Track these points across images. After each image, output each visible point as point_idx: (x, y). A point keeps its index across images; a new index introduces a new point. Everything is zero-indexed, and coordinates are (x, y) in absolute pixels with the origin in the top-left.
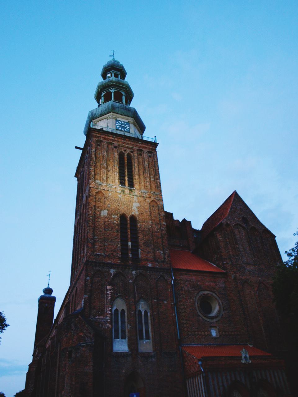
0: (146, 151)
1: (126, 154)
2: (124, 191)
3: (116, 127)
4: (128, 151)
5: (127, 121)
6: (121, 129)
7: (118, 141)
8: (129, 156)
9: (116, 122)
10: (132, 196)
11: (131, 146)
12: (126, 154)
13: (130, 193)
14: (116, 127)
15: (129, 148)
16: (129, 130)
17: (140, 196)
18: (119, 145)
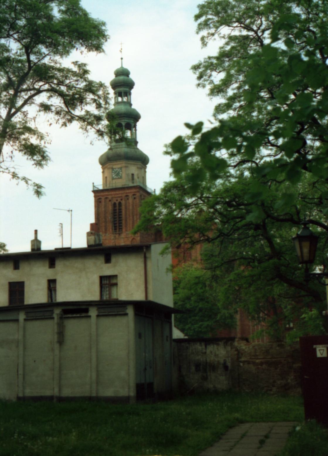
0: (130, 195)
1: (117, 203)
2: (115, 237)
4: (119, 200)
5: (119, 166)
7: (111, 195)
8: (120, 203)
11: (120, 195)
12: (117, 203)
15: (119, 197)
18: (112, 198)
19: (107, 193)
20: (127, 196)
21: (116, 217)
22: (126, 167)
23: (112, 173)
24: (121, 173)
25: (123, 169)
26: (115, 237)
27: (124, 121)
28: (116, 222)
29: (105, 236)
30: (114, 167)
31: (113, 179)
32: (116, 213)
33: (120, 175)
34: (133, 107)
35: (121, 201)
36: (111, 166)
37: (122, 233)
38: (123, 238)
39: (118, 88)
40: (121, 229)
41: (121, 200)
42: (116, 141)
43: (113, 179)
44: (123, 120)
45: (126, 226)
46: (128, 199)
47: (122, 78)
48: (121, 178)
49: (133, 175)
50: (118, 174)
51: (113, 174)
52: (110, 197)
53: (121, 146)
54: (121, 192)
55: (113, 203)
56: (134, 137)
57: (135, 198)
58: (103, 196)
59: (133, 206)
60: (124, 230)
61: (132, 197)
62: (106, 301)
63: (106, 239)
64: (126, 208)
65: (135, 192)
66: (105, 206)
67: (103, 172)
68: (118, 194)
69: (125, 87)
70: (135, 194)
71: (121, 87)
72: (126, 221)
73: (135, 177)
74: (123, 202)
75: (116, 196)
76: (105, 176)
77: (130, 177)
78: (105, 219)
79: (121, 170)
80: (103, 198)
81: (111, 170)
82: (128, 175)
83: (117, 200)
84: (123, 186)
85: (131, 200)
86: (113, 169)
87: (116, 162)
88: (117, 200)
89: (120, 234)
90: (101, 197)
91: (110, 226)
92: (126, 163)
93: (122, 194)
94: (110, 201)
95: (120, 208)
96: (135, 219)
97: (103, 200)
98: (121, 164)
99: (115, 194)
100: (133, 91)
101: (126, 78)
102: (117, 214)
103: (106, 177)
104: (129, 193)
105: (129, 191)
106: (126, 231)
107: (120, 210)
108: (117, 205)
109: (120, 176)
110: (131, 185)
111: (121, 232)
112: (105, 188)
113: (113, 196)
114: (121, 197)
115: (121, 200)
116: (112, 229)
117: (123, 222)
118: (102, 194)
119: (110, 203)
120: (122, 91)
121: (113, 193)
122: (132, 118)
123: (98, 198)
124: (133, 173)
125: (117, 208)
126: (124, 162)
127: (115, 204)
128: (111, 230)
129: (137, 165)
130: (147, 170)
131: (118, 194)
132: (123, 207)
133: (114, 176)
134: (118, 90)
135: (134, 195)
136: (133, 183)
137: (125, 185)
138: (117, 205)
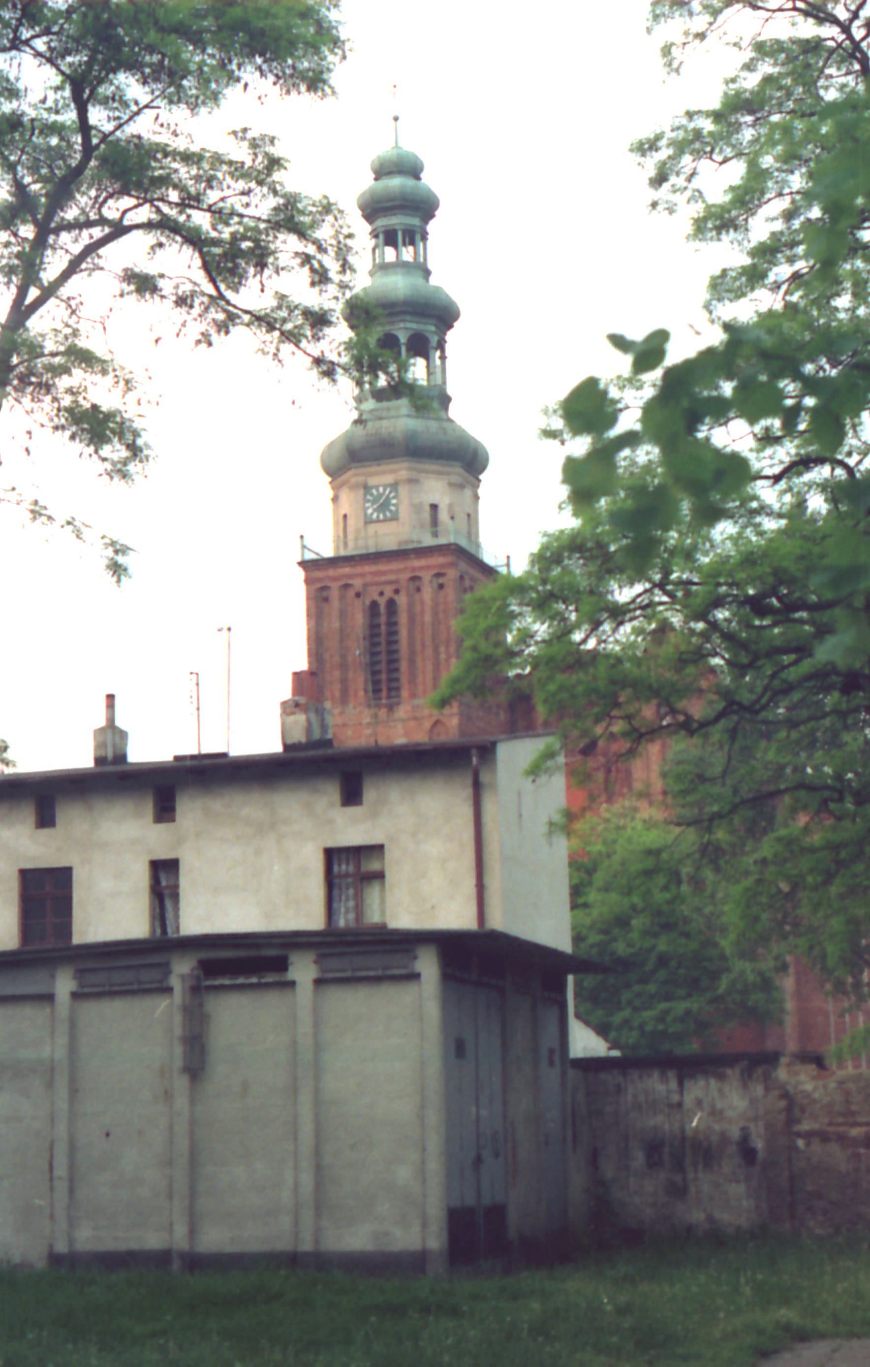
0: (427, 576)
1: (382, 602)
2: (376, 716)
3: (365, 514)
4: (388, 591)
5: (389, 479)
6: (378, 516)
7: (362, 575)
8: (391, 603)
9: (365, 495)
10: (392, 724)
11: (392, 577)
12: (382, 602)
13: (388, 717)
14: (365, 514)
15: (390, 583)
16: (397, 511)
17: (408, 719)
18: (365, 586)
19: (347, 570)
20: (414, 579)
21: (378, 649)
22: (412, 481)
23: (366, 501)
24: (394, 501)
25: (403, 490)
26: (376, 716)
27: (407, 329)
28: (377, 668)
29: (342, 713)
30: (372, 481)
31: (368, 521)
32: (379, 635)
33: (393, 508)
34: (434, 281)
35: (396, 597)
36: (361, 479)
37: (398, 704)
38: (402, 720)
39: (385, 216)
40: (394, 689)
41: (397, 591)
42: (379, 395)
43: (368, 521)
44: (402, 325)
45: (412, 681)
46: (418, 590)
47: (395, 182)
48: (395, 518)
49: (434, 507)
50: (384, 506)
51: (368, 505)
52: (357, 583)
53: (392, 413)
54: (394, 566)
55: (368, 602)
56: (439, 381)
57: (441, 586)
58: (335, 579)
59: (435, 614)
60: (405, 693)
61: (431, 582)
62: (347, 932)
63: (345, 725)
64: (412, 619)
65: (443, 566)
66: (343, 614)
67: (335, 499)
68: (384, 573)
69: (406, 215)
70: (442, 571)
71: (395, 215)
72: (412, 662)
73: (443, 516)
74: (402, 600)
75: (377, 579)
76: (343, 512)
77: (426, 514)
78: (343, 657)
79: (396, 491)
80: (335, 586)
81: (362, 492)
82: (417, 508)
83: (381, 594)
84: (403, 547)
85: (427, 593)
86: (366, 488)
87: (379, 465)
88: (381, 594)
89: (391, 708)
90: (329, 584)
91: (359, 680)
92: (409, 469)
93: (398, 571)
94: (358, 595)
95: (394, 620)
96: (443, 657)
97: (334, 594)
98: (393, 471)
99: (374, 574)
100: (432, 227)
101: (410, 182)
102: (383, 640)
103: (345, 516)
104: (421, 568)
105: (422, 562)
106: (413, 696)
107: (392, 625)
108: (383, 609)
109: (391, 511)
110: (428, 541)
111: (395, 700)
112: (343, 553)
113: (369, 579)
114: (397, 582)
115: (397, 591)
116: (366, 691)
117: (404, 666)
118: (331, 572)
119: (358, 603)
120: (396, 227)
121: (367, 569)
122: (429, 316)
123: (319, 585)
124: (435, 502)
125: (383, 619)
126: (406, 464)
127: (374, 605)
128: (361, 693)
129: (448, 474)
130: (481, 491)
131: (384, 573)
132: (403, 618)
133: (370, 511)
134: (382, 222)
135: (438, 575)
136: (435, 535)
137: (407, 542)
138: (383, 609)
